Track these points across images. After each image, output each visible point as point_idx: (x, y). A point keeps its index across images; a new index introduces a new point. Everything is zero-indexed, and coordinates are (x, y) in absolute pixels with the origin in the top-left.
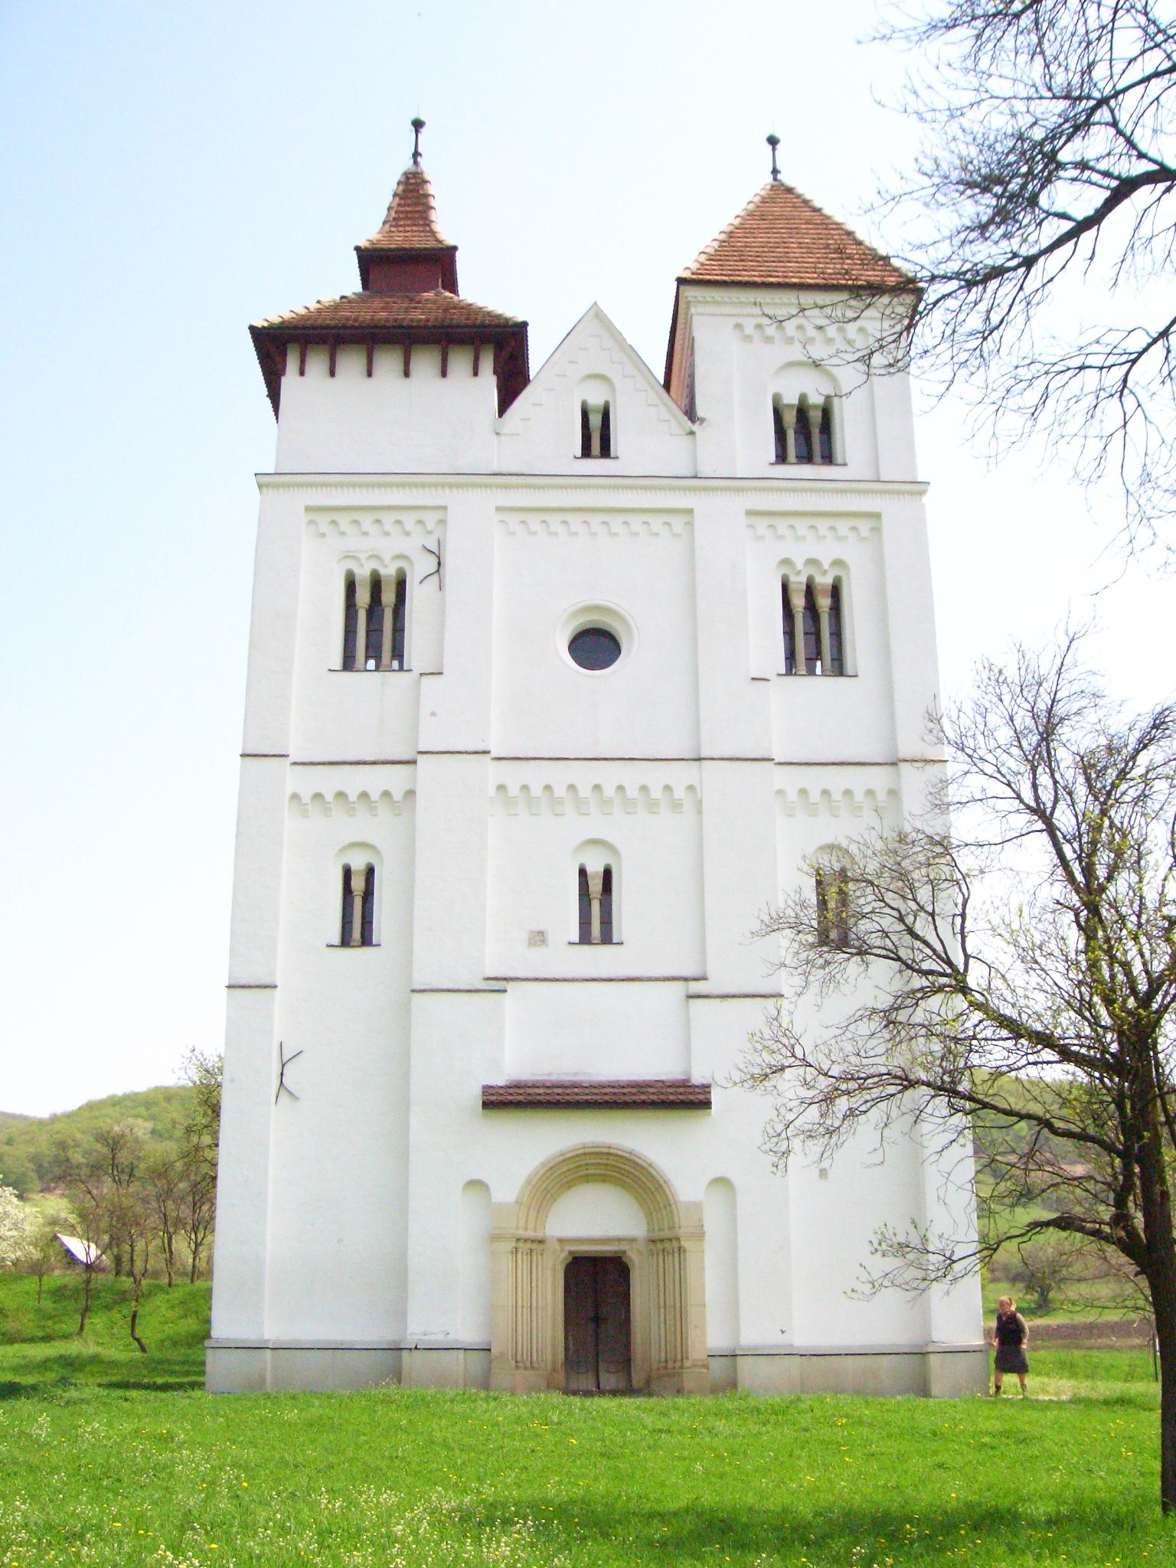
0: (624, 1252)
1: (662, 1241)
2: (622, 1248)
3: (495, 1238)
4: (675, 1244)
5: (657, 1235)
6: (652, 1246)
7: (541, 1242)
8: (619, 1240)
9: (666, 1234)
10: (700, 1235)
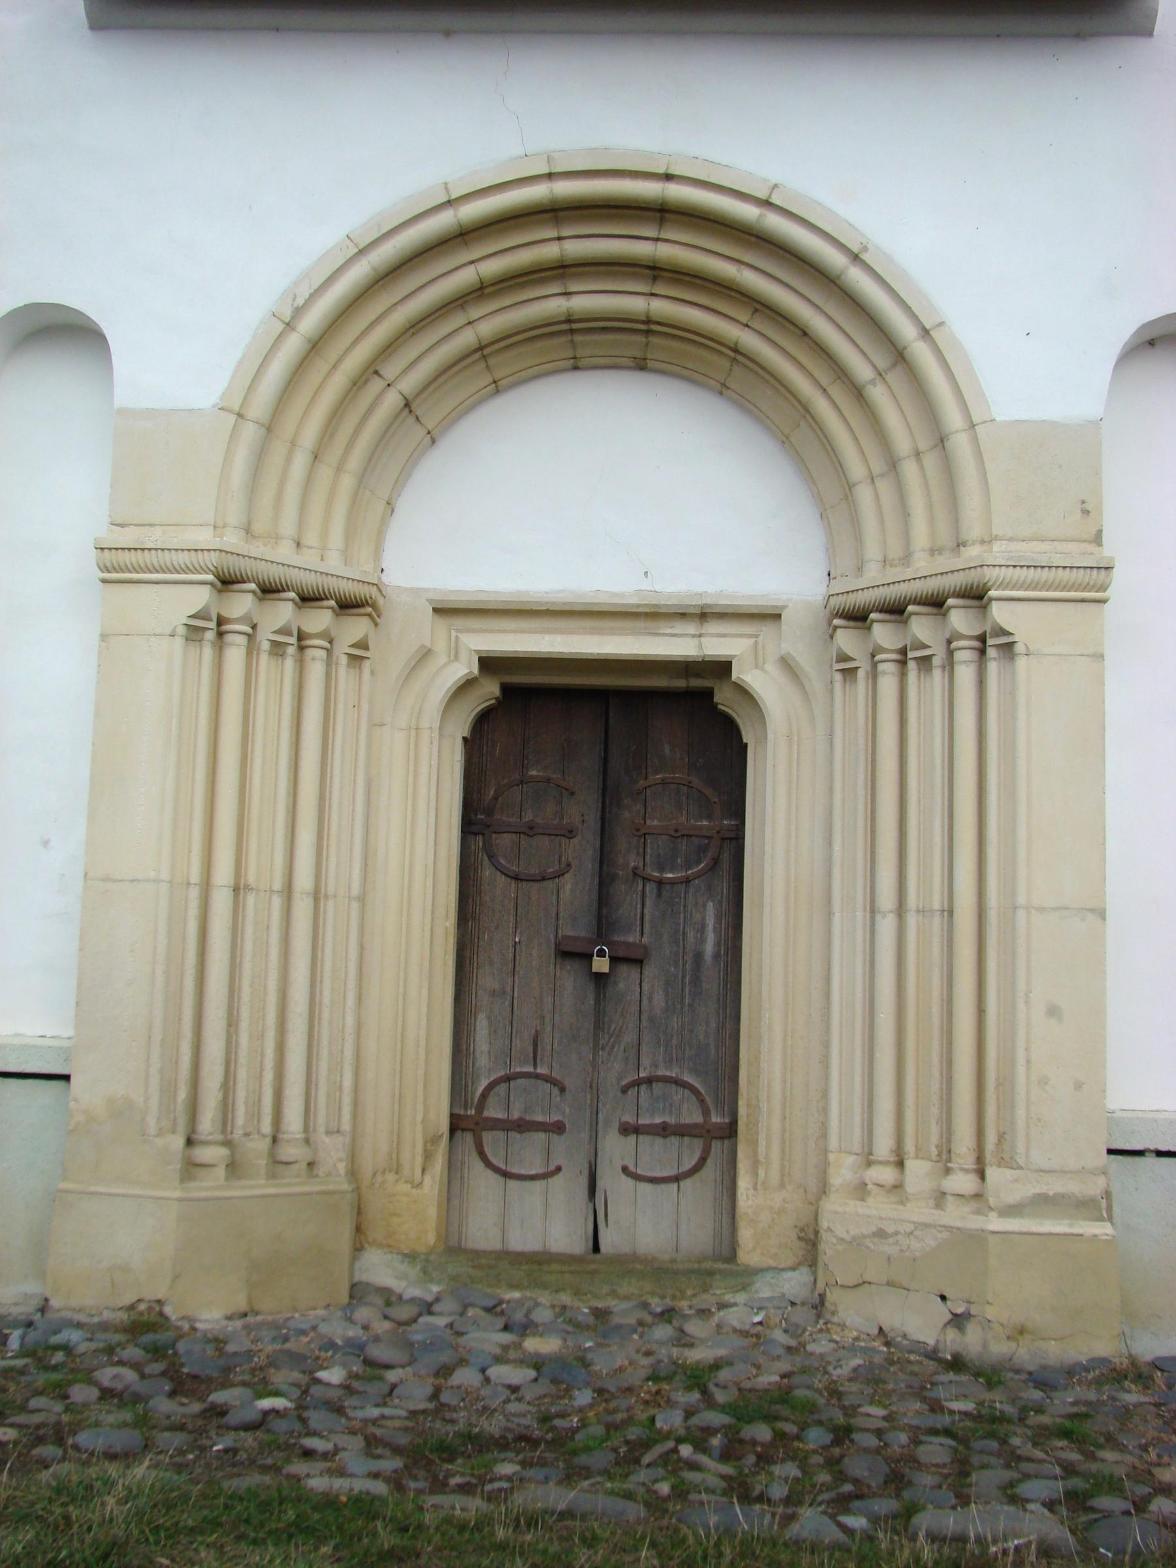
0: (723, 668)
1: (896, 610)
2: (715, 644)
3: (120, 568)
4: (960, 619)
5: (875, 581)
6: (847, 640)
7: (347, 606)
8: (704, 615)
9: (925, 570)
10: (1088, 586)
